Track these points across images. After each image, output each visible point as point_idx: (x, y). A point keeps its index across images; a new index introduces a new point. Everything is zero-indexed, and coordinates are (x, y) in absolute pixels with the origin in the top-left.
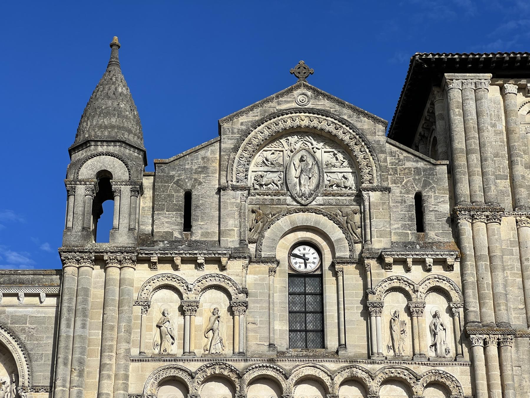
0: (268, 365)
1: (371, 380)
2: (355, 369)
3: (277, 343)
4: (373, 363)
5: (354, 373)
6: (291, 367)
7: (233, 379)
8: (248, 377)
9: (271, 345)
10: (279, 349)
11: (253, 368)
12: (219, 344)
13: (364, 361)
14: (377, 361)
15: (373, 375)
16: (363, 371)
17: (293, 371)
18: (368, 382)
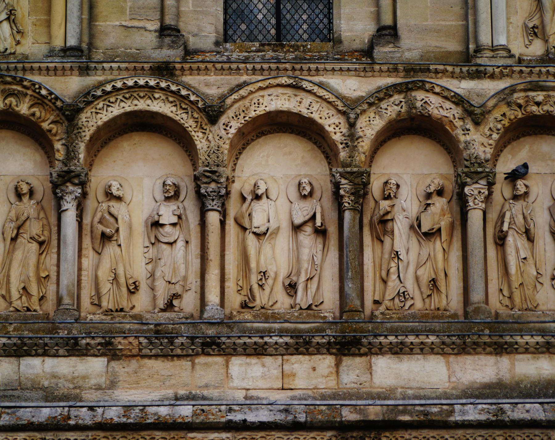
0: (152, 83)
1: (470, 126)
2: (420, 95)
3: (188, 26)
4: (478, 74)
5: (419, 104)
6: (224, 90)
7: (45, 126)
8: (92, 120)
9: (168, 32)
10: (193, 42)
11: (105, 93)
12: (6, 26)
13: (450, 68)
14: (490, 69)
15: (478, 111)
16: (446, 98)
17: (229, 101)
18: (459, 132)
